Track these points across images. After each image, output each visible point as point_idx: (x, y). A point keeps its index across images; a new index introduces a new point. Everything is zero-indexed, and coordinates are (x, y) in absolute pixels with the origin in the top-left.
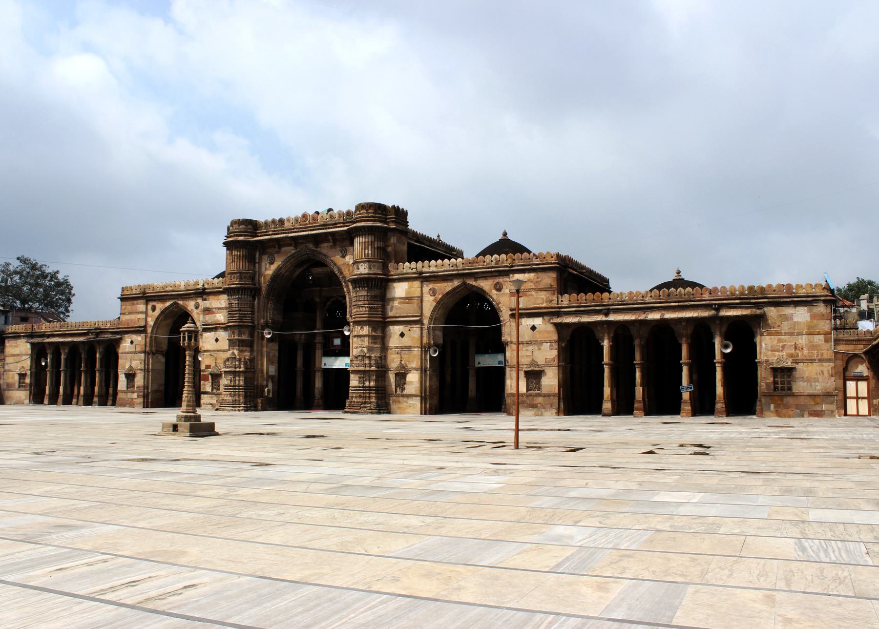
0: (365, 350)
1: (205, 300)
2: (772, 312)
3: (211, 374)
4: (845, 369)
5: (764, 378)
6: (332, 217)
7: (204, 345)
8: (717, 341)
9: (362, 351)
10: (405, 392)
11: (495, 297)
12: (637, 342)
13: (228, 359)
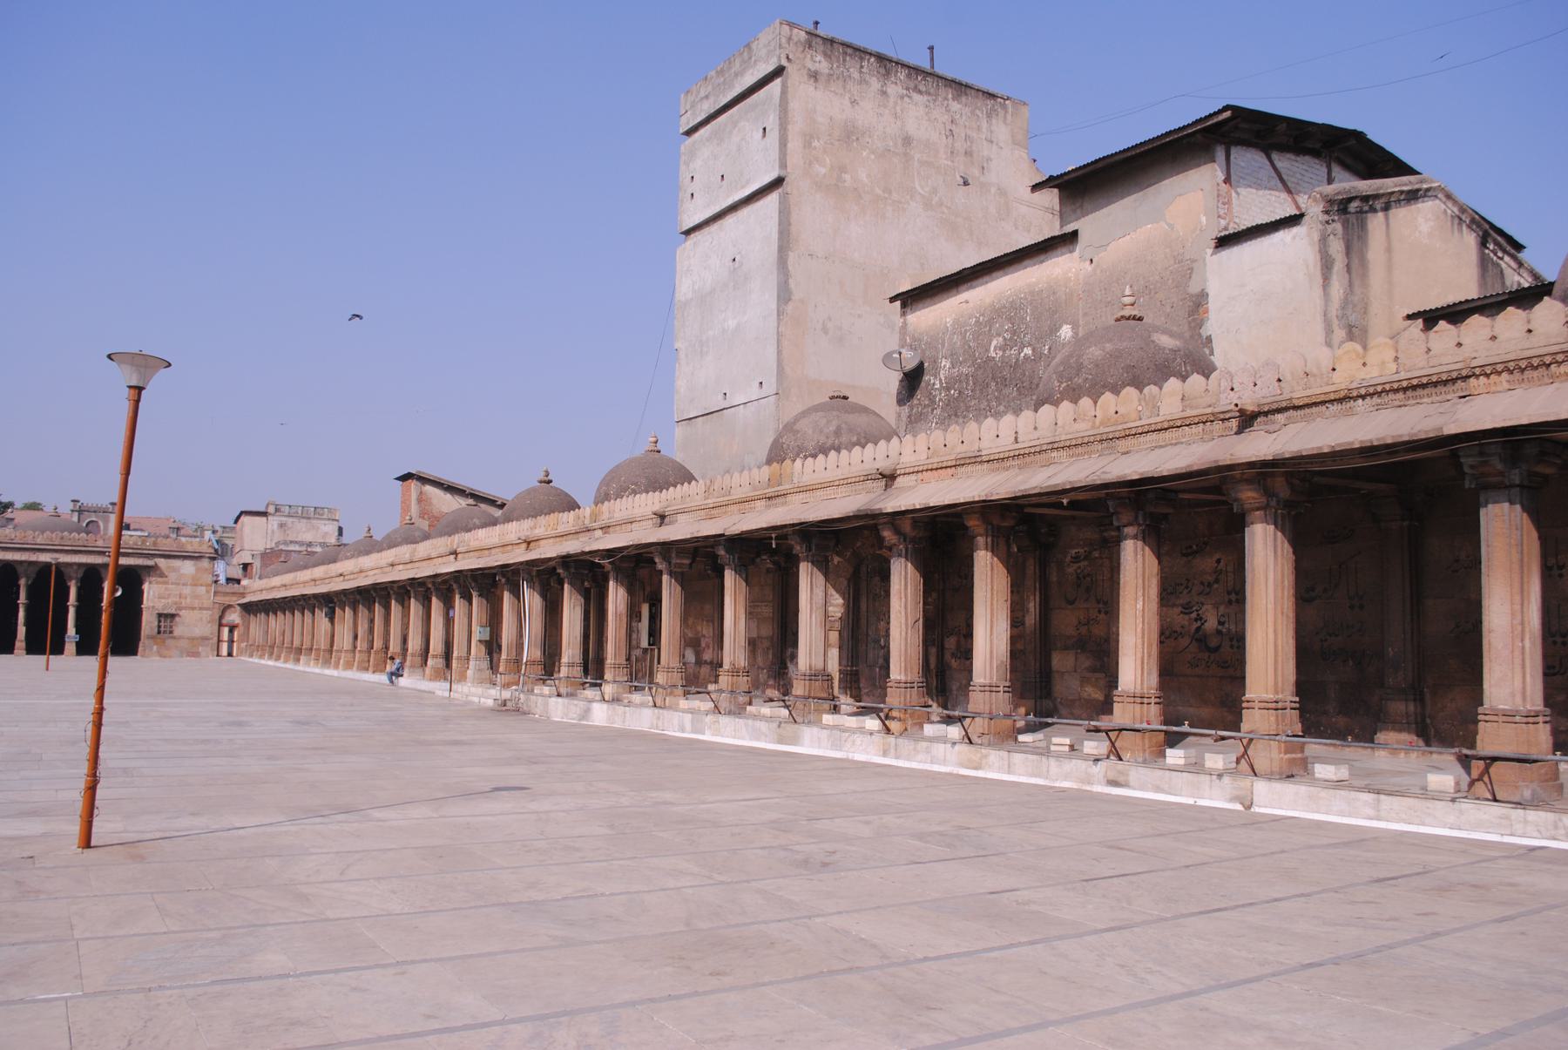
2: (162, 562)
4: (221, 618)
5: (148, 622)
8: (106, 586)
12: (22, 582)
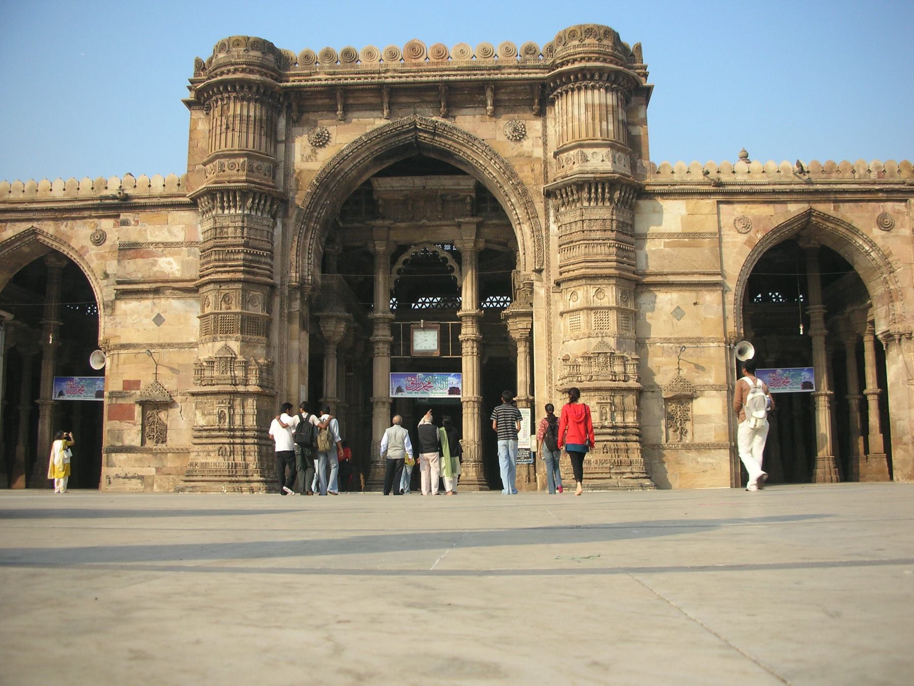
0: (612, 342)
1: (125, 223)
3: (144, 404)
6: (487, 53)
7: (120, 331)
9: (603, 343)
10: (688, 439)
11: (879, 242)
13: (211, 362)
